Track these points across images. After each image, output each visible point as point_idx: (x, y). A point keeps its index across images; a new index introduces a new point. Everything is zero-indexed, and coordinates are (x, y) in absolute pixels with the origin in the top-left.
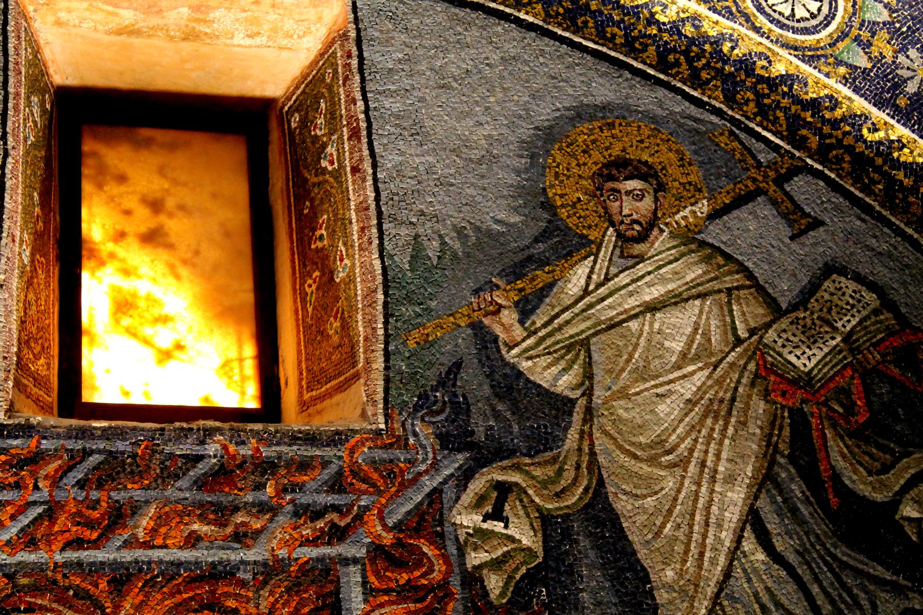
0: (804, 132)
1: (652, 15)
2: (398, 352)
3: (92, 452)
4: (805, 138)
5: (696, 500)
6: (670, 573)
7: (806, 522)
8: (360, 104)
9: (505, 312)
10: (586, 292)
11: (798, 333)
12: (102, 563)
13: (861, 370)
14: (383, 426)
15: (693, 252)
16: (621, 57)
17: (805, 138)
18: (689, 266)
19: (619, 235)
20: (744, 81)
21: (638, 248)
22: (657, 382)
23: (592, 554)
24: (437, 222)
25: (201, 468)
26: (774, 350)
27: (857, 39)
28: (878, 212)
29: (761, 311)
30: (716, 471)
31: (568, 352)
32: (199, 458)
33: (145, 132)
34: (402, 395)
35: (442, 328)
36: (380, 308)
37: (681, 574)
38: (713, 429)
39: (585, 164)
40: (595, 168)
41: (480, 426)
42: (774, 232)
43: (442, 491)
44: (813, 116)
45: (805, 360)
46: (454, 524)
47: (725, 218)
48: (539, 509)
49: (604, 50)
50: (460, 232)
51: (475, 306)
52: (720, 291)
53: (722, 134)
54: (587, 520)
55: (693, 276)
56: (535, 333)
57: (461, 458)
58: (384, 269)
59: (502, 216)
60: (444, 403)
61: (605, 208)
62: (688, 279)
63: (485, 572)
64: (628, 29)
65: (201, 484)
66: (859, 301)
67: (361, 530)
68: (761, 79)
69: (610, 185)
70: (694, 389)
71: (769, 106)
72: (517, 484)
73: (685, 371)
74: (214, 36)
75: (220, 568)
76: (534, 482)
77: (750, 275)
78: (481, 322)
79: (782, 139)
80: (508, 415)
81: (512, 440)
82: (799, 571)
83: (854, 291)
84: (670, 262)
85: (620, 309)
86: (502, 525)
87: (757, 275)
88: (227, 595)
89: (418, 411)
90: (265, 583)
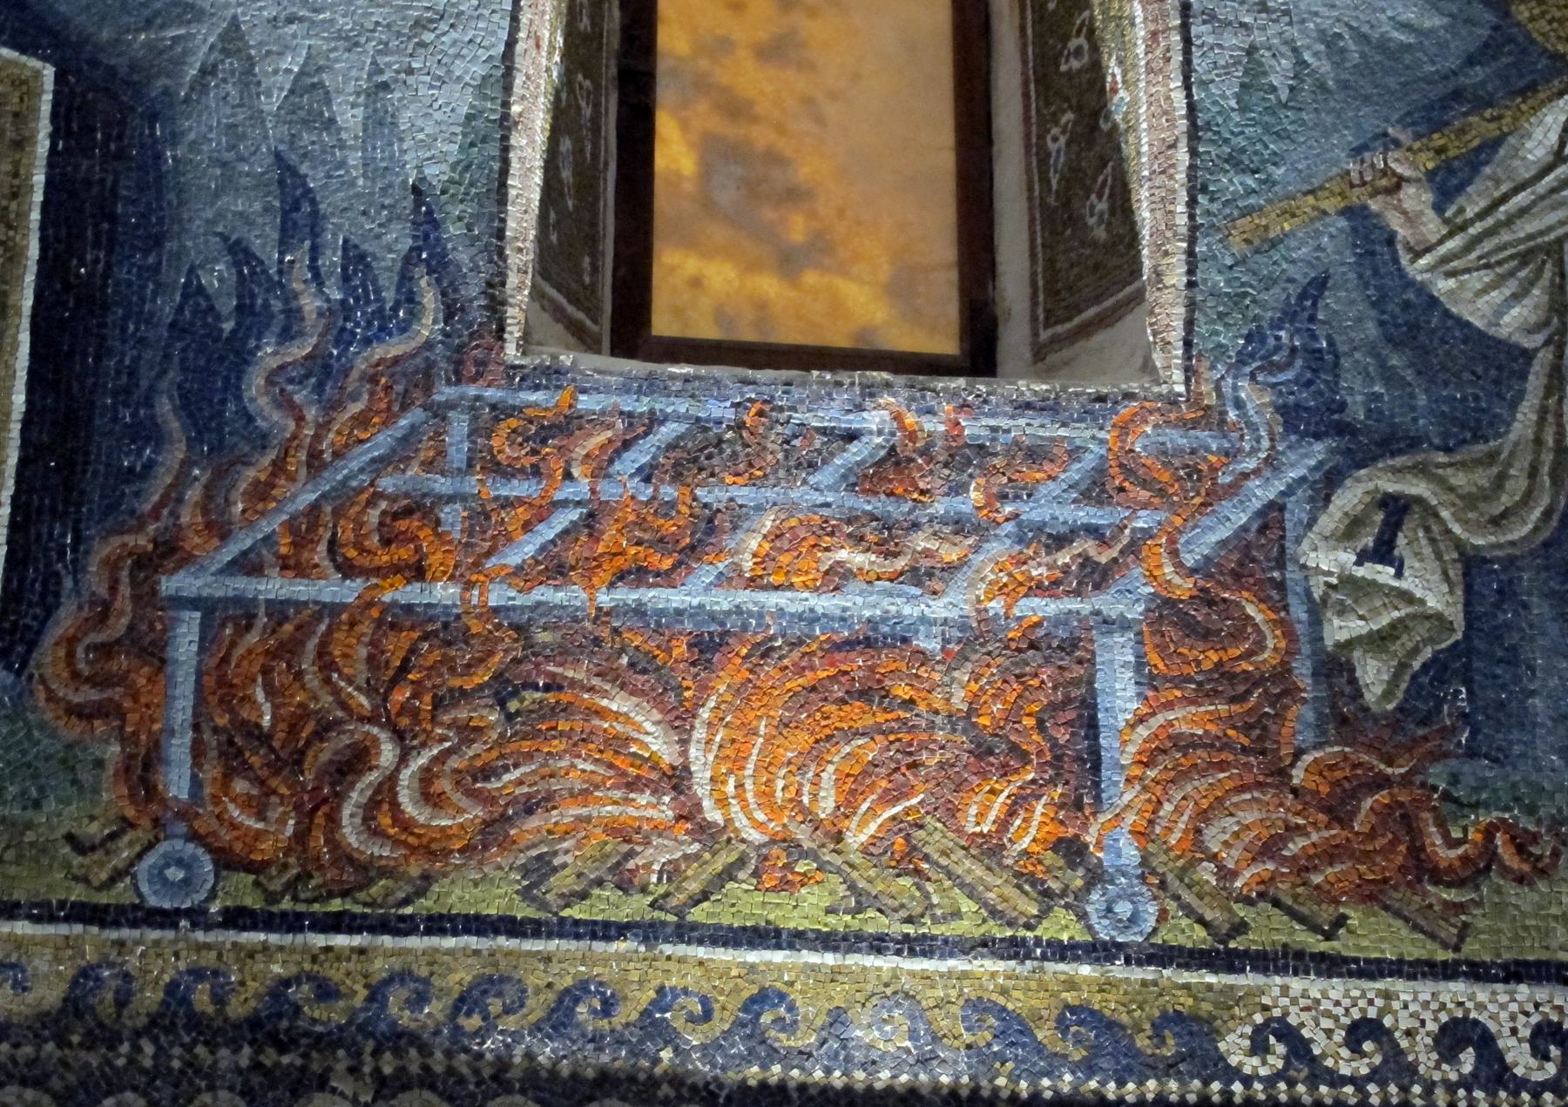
9: (1409, 191)
12: (679, 612)
14: (1180, 388)
24: (1290, 23)
25: (855, 452)
32: (852, 436)
34: (1217, 333)
35: (1293, 215)
36: (1181, 177)
41: (1357, 395)
43: (1282, 509)
46: (1304, 567)
48: (1458, 545)
50: (1331, 42)
51: (1355, 176)
54: (1547, 569)
56: (1463, 228)
57: (1319, 450)
58: (1192, 108)
59: (1410, 15)
60: (1293, 350)
63: (1357, 654)
72: (1419, 500)
76: (1452, 497)
78: (1365, 207)
80: (1409, 375)
81: (1415, 420)
86: (1392, 571)
89: (1245, 364)
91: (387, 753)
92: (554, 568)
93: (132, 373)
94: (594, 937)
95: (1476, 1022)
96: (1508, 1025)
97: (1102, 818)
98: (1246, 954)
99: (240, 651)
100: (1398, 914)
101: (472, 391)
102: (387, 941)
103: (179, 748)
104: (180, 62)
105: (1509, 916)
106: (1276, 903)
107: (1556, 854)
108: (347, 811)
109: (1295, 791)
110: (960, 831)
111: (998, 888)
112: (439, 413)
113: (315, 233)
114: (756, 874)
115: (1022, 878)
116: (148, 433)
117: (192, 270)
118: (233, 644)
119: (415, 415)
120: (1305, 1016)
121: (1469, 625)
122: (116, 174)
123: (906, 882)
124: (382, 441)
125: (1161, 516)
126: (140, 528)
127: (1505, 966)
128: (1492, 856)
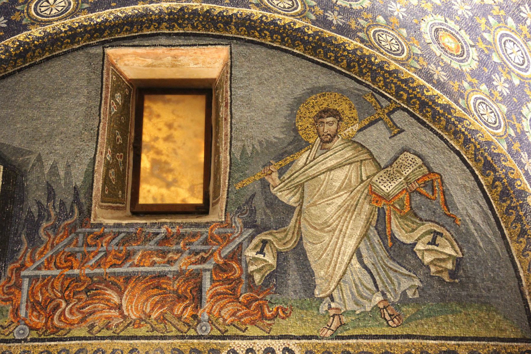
0: (402, 92)
1: (345, 47)
2: (232, 191)
3: (121, 233)
4: (402, 95)
5: (336, 244)
6: (322, 273)
7: (378, 252)
8: (229, 93)
9: (274, 174)
10: (305, 164)
11: (387, 177)
12: (122, 272)
13: (409, 191)
14: (223, 220)
15: (349, 146)
16: (332, 65)
17: (402, 95)
18: (347, 152)
19: (321, 140)
20: (380, 73)
21: (328, 145)
22: (328, 199)
23: (294, 266)
25: (159, 237)
26: (376, 184)
27: (414, 58)
28: (428, 125)
29: (373, 168)
30: (346, 233)
31: (296, 188)
32: (158, 234)
33: (168, 97)
37: (326, 273)
38: (347, 217)
39: (312, 112)
40: (316, 113)
42: (383, 136)
43: (242, 244)
44: (405, 86)
45: (388, 188)
47: (364, 131)
48: (277, 250)
49: (326, 63)
50: (260, 143)
52: (358, 161)
53: (368, 95)
55: (348, 155)
56: (284, 181)
57: (251, 231)
59: (277, 135)
61: (317, 130)
62: (346, 156)
63: (254, 273)
64: (336, 53)
65: (158, 243)
66: (414, 162)
67: (212, 259)
68: (386, 72)
69: (321, 120)
70: (342, 201)
71: (389, 83)
72: (270, 240)
73: (339, 194)
74: (181, 65)
75: (162, 273)
77: (371, 154)
78: (264, 178)
79: (392, 96)
82: (372, 271)
83: (412, 159)
84: (340, 151)
85: (318, 171)
87: (374, 154)
88: (163, 283)
90: (177, 278)
91: (64, 305)
92: (98, 265)
93: (17, 230)
94: (101, 339)
95: (272, 348)
96: (278, 348)
97: (201, 310)
98: (227, 336)
99: (36, 286)
100: (258, 327)
101: (84, 229)
102: (61, 343)
103: (23, 307)
104: (28, 164)
105: (281, 326)
106: (234, 326)
107: (290, 313)
108: (55, 317)
109: (240, 302)
110: (173, 314)
111: (181, 326)
112: (77, 234)
113: (54, 198)
114: (133, 325)
115: (185, 323)
116: (20, 242)
117: (29, 208)
118: (35, 285)
119: (73, 235)
120: (238, 348)
121: (277, 266)
122: (15, 188)
123: (162, 325)
124: (66, 241)
125: (218, 247)
126: (17, 262)
127: (278, 336)
128: (277, 313)
